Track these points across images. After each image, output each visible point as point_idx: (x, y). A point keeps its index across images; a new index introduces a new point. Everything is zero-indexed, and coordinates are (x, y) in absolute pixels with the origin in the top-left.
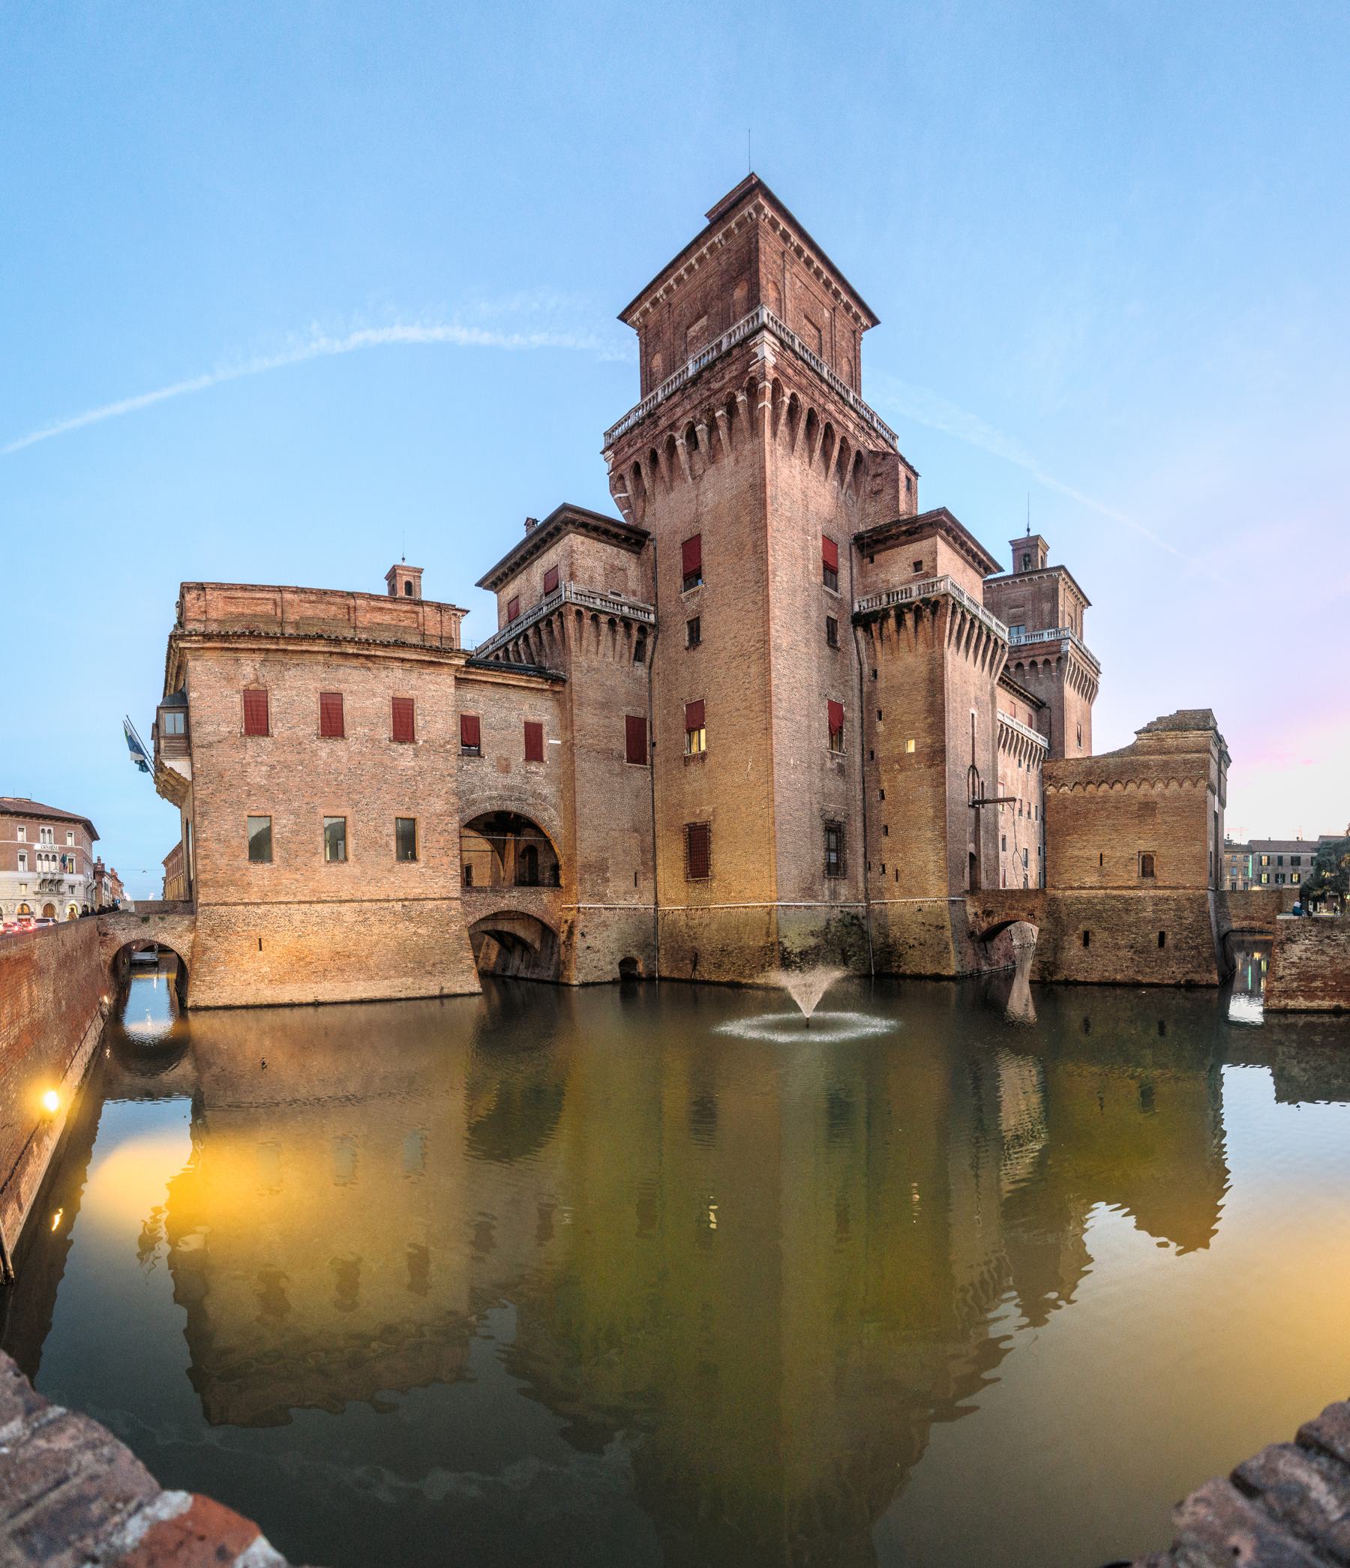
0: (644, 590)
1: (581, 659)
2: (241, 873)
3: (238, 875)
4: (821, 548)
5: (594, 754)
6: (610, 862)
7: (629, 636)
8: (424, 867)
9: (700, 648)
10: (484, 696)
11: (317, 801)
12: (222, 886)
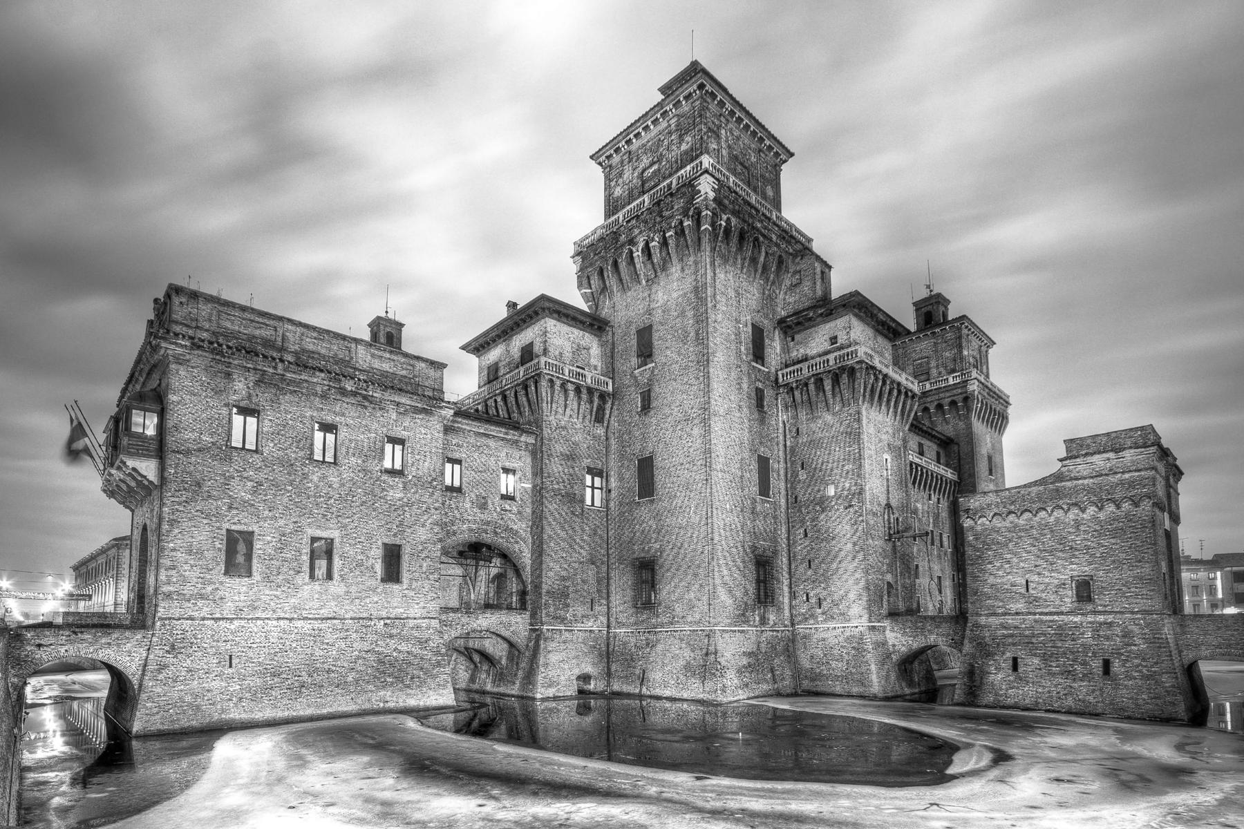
0: (604, 366)
1: (550, 419)
2: (213, 587)
3: (209, 589)
4: (751, 333)
5: (559, 497)
6: (571, 589)
7: (591, 402)
8: (407, 589)
9: (652, 412)
10: (467, 443)
11: (305, 521)
12: (189, 601)
